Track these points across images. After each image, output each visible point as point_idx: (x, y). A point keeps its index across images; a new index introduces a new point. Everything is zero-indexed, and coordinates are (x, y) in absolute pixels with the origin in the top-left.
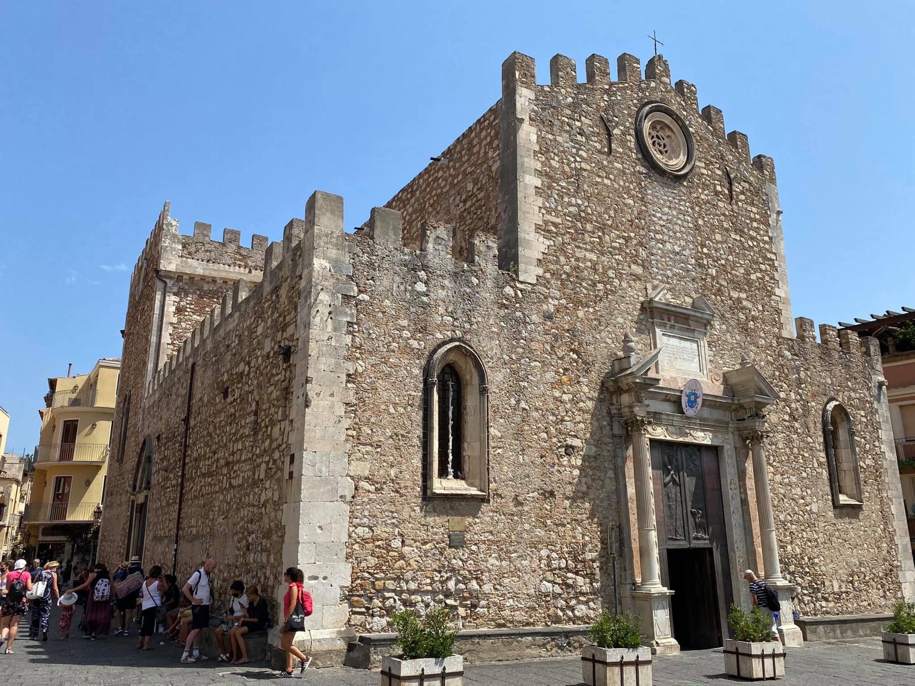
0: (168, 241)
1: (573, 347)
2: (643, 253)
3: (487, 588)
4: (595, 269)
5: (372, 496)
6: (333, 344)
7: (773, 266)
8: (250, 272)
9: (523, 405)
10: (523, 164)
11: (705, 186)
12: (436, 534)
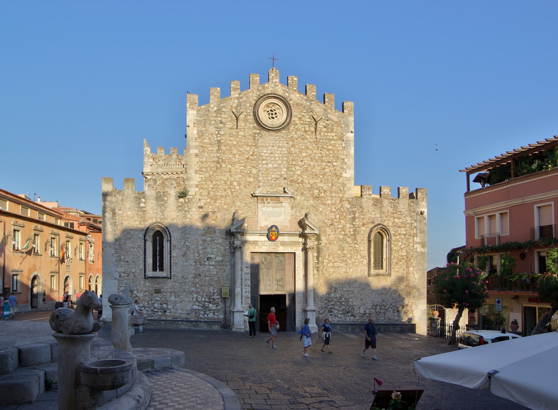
1: (212, 219)
2: (254, 171)
3: (170, 307)
5: (125, 278)
7: (343, 162)
10: (189, 145)
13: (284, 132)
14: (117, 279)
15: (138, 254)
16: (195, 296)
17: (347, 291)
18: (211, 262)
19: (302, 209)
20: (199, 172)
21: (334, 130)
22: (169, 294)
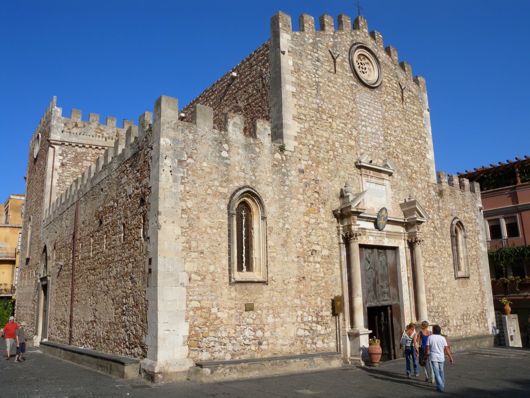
0: (55, 121)
1: (315, 190)
3: (267, 334)
4: (327, 142)
6: (173, 191)
7: (426, 142)
8: (106, 140)
9: (287, 226)
11: (388, 94)
12: (237, 304)
13: (377, 91)
14: (185, 285)
15: (219, 239)
16: (300, 313)
17: (442, 298)
18: (316, 257)
19: (400, 190)
20: (297, 120)
21: (415, 103)
22: (265, 311)
